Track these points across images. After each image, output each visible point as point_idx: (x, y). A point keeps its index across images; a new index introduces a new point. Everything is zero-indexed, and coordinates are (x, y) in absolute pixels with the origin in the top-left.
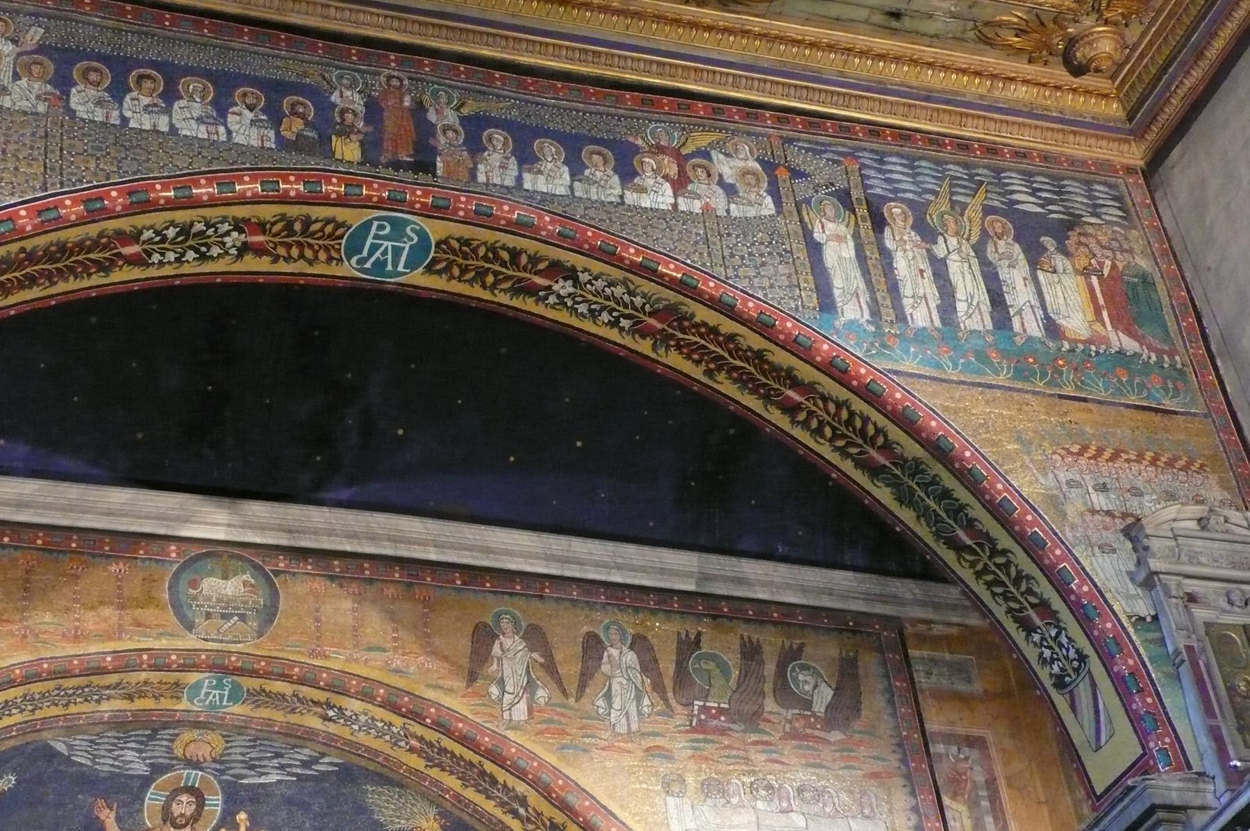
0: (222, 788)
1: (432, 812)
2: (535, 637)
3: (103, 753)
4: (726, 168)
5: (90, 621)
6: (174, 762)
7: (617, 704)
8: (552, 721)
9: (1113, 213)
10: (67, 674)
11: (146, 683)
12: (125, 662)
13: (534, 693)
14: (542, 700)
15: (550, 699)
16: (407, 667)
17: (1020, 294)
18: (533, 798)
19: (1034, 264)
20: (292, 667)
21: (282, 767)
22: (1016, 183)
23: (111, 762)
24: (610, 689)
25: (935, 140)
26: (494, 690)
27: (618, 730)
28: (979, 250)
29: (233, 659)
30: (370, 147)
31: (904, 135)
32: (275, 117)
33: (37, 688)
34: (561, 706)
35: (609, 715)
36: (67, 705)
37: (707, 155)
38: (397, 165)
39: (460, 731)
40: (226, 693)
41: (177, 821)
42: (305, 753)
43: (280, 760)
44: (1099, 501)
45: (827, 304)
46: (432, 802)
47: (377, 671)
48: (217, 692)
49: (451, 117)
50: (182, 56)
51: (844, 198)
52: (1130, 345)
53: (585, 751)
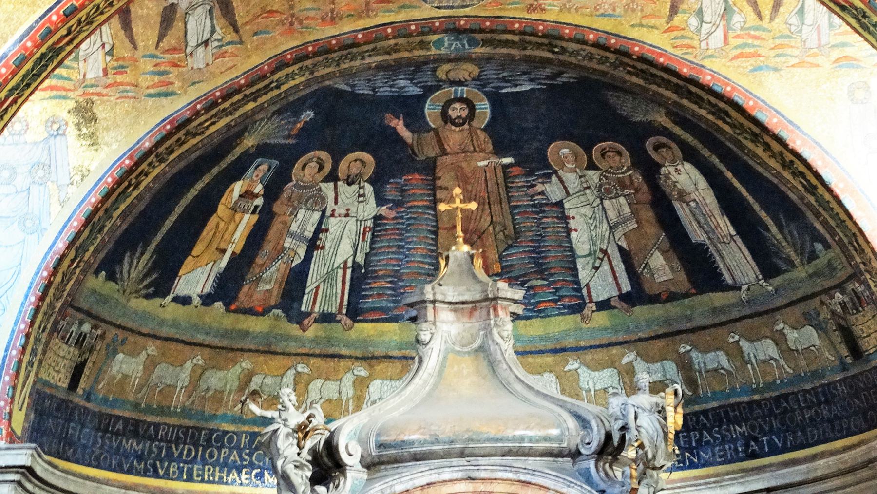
0: (487, 97)
1: (663, 111)
3: (381, 85)
6: (441, 84)
7: (809, 18)
8: (746, 45)
10: (329, 51)
11: (396, 44)
12: (375, 35)
13: (731, 17)
14: (738, 26)
15: (745, 22)
16: (614, 10)
18: (732, 112)
20: (513, 23)
21: (531, 80)
23: (389, 89)
24: (802, 7)
26: (694, 22)
27: (808, 45)
29: (462, 23)
33: (309, 63)
34: (757, 29)
35: (801, 31)
36: (338, 65)
39: (662, 64)
40: (465, 42)
41: (456, 121)
42: (548, 71)
43: (527, 76)
46: (660, 105)
47: (587, 18)
48: (458, 43)
53: (776, 70)
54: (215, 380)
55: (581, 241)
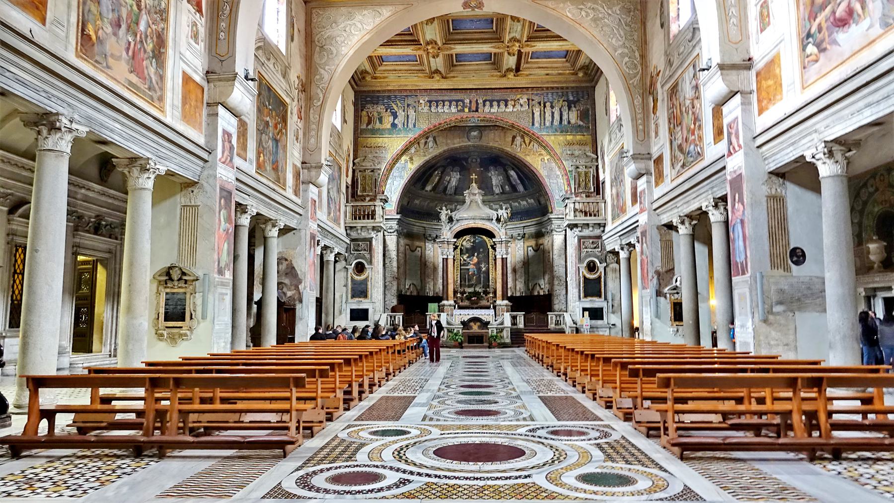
2: (522, 137)
4: (521, 101)
5: (455, 141)
9: (586, 97)
12: (461, 147)
17: (565, 117)
19: (569, 110)
22: (570, 95)
25: (557, 88)
28: (560, 109)
30: (470, 109)
31: (552, 88)
32: (457, 106)
37: (519, 99)
38: (473, 111)
44: (569, 152)
45: (533, 124)
49: (481, 101)
50: (446, 98)
51: (540, 103)
52: (581, 123)
54: (431, 205)
55: (494, 183)
